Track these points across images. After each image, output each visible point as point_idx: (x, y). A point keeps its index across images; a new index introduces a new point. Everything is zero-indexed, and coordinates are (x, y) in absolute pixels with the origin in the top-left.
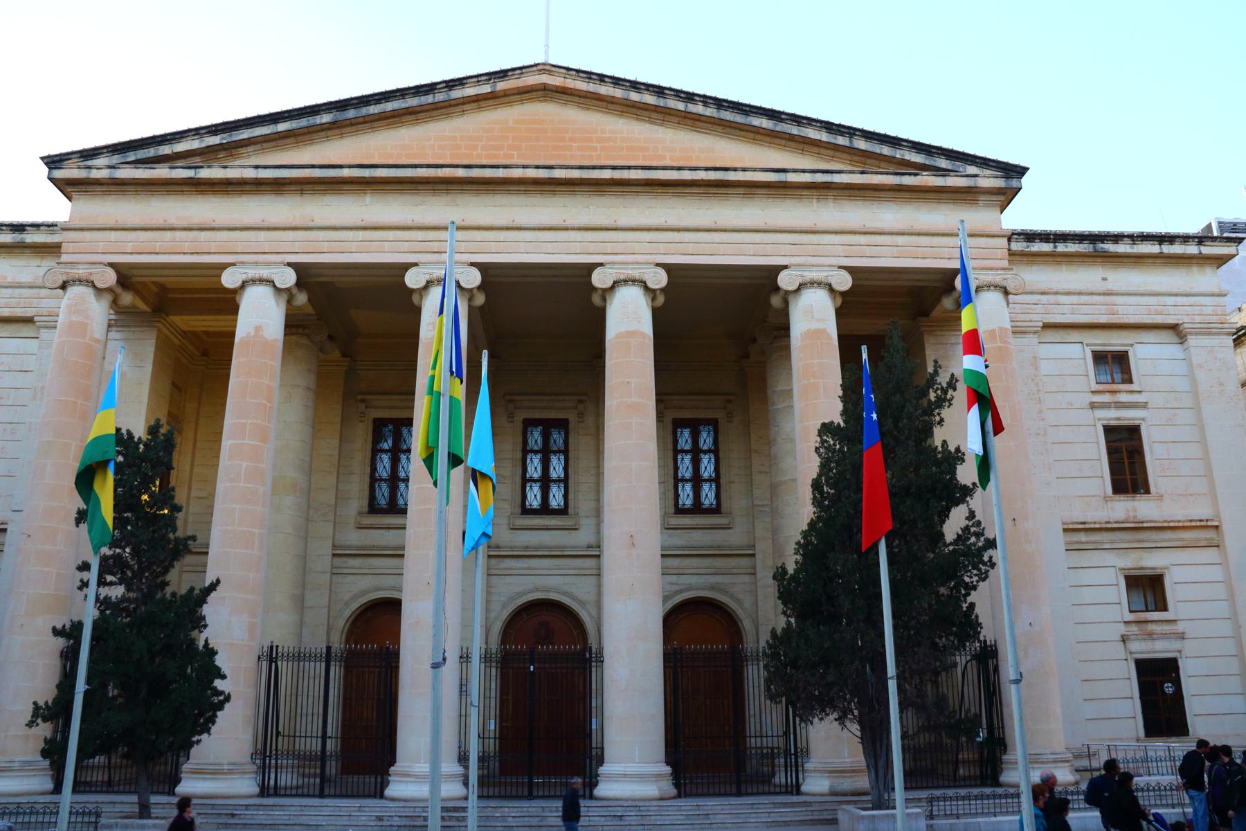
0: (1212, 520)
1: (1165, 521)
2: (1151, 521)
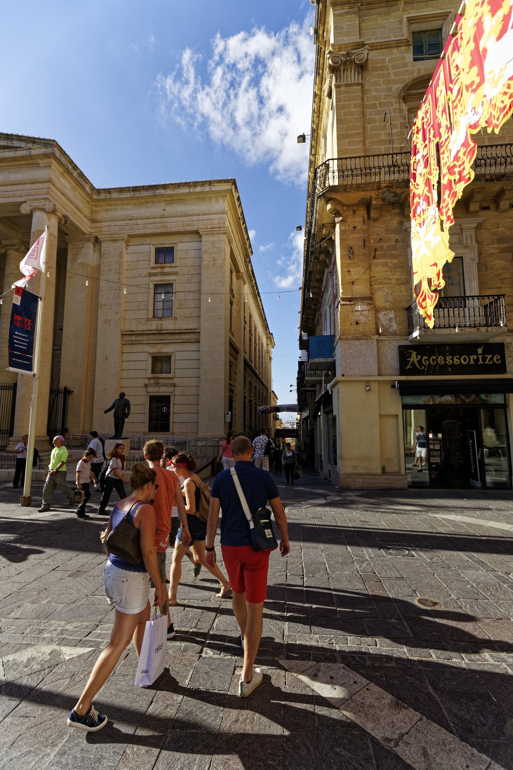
0: (197, 329)
1: (172, 330)
2: (166, 330)
